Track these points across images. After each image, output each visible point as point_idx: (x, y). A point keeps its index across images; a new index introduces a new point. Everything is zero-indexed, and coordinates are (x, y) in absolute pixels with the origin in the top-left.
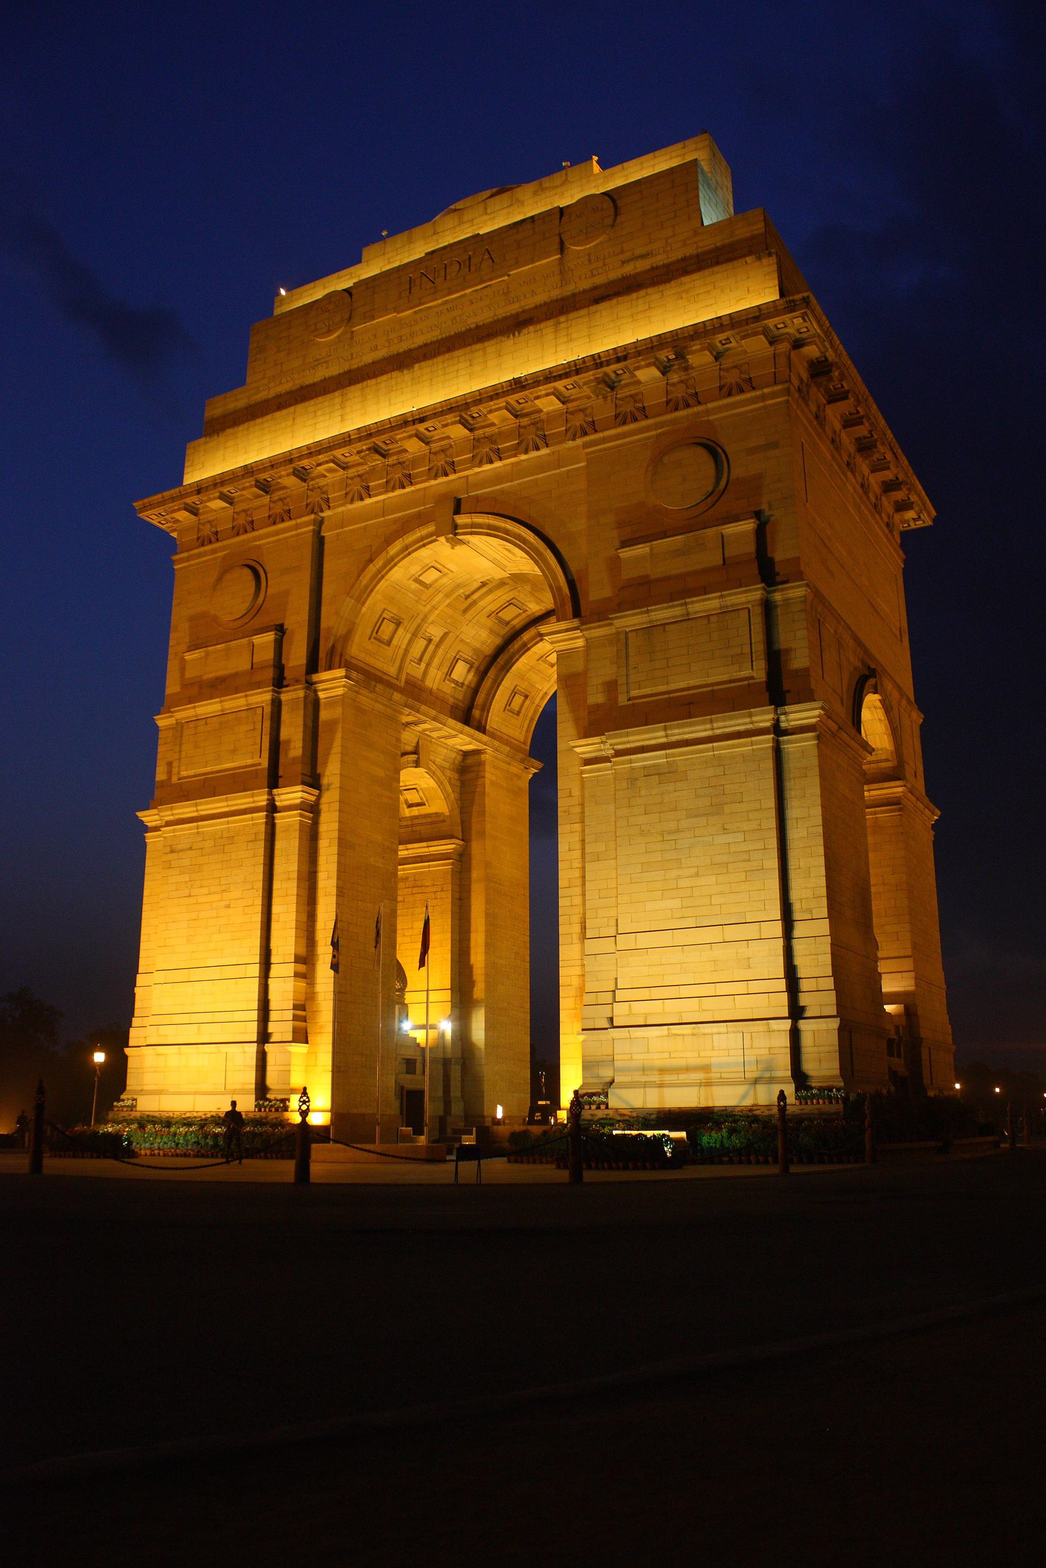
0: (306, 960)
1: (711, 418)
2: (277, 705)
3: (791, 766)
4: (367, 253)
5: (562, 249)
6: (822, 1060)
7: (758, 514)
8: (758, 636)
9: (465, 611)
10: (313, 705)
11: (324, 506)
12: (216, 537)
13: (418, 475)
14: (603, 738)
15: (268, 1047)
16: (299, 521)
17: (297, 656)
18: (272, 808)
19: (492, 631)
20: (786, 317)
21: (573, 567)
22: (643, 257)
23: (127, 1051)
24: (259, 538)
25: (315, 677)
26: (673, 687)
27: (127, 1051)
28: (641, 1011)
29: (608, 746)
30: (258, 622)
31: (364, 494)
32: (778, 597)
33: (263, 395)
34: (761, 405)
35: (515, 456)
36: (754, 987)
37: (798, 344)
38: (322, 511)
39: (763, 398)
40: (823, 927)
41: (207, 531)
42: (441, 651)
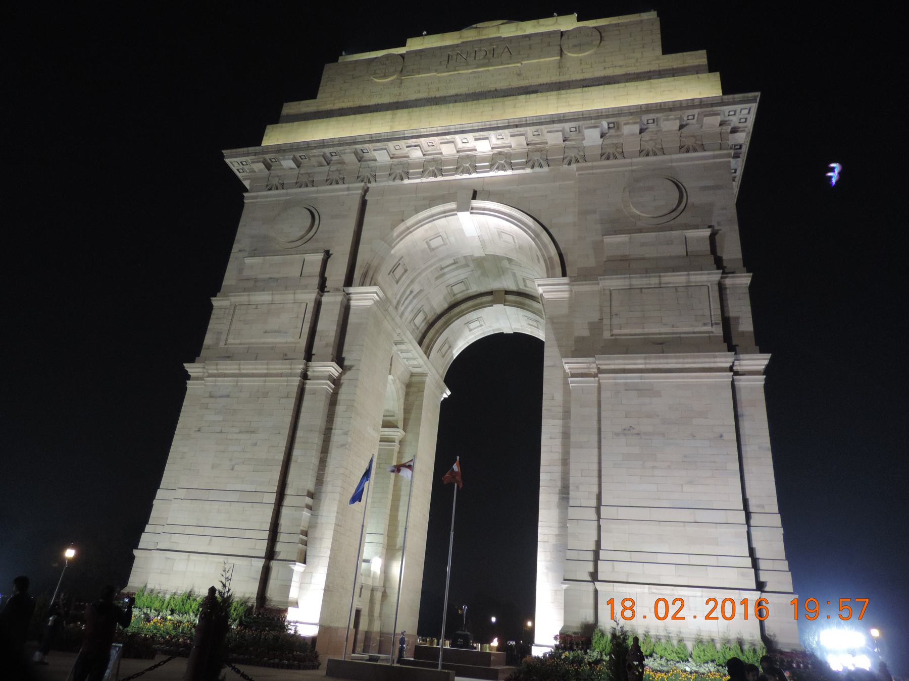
1: (674, 164)
2: (318, 304)
3: (743, 396)
4: (410, 41)
5: (561, 53)
7: (710, 227)
9: (437, 278)
10: (346, 309)
11: (372, 179)
12: (283, 186)
14: (591, 359)
16: (351, 185)
17: (337, 272)
18: (305, 376)
19: (445, 298)
20: (738, 107)
21: (561, 246)
22: (621, 66)
23: (136, 552)
24: (317, 192)
25: (351, 290)
26: (646, 331)
27: (136, 552)
28: (622, 571)
29: (594, 365)
32: (728, 282)
33: (328, 107)
34: (712, 161)
35: (523, 169)
37: (734, 130)
38: (370, 182)
39: (715, 157)
40: (777, 520)
41: (275, 181)
42: (415, 301)
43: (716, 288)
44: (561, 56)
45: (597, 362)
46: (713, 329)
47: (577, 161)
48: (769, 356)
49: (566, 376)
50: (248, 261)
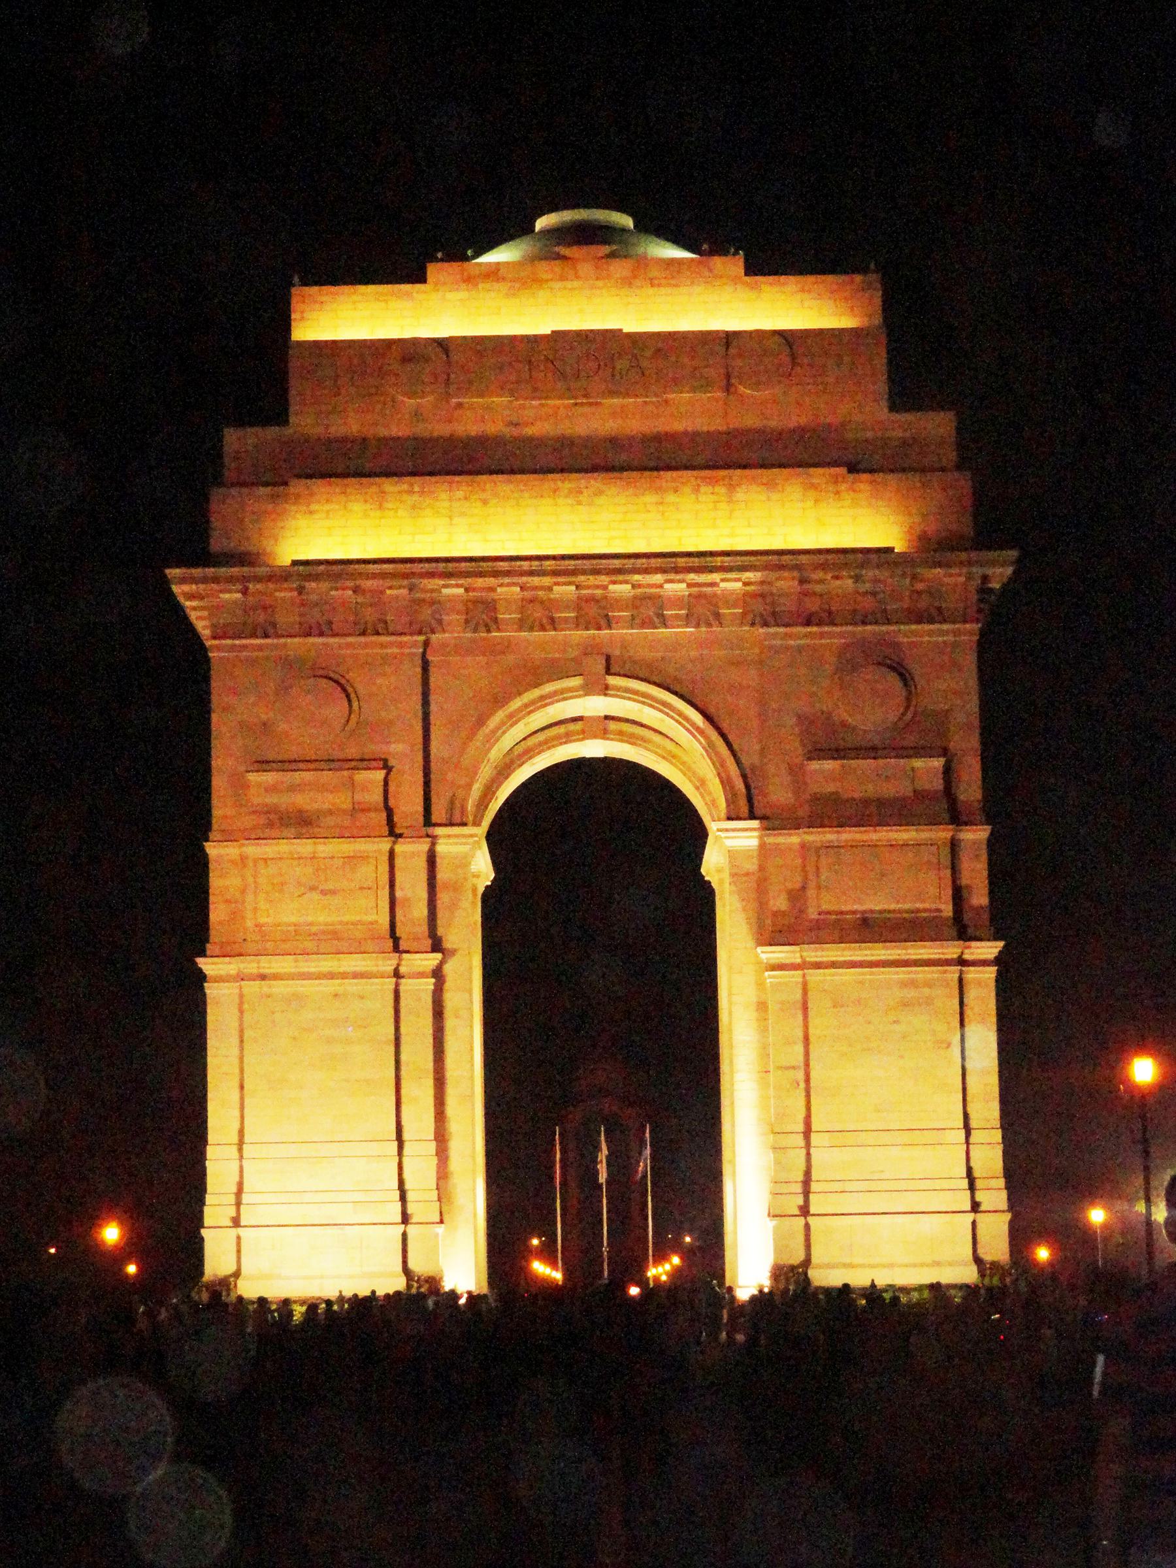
0: (441, 1138)
3: (971, 995)
4: (432, 269)
6: (997, 1248)
7: (945, 752)
8: (948, 873)
10: (432, 860)
13: (566, 620)
14: (796, 948)
15: (412, 1230)
17: (409, 804)
25: (439, 831)
27: (204, 1232)
29: (798, 955)
30: (352, 751)
31: (491, 624)
36: (938, 1184)
38: (433, 632)
40: (997, 1136)
43: (948, 850)
44: (728, 388)
45: (805, 954)
46: (943, 907)
47: (766, 624)
48: (1001, 944)
49: (760, 963)
50: (252, 777)
